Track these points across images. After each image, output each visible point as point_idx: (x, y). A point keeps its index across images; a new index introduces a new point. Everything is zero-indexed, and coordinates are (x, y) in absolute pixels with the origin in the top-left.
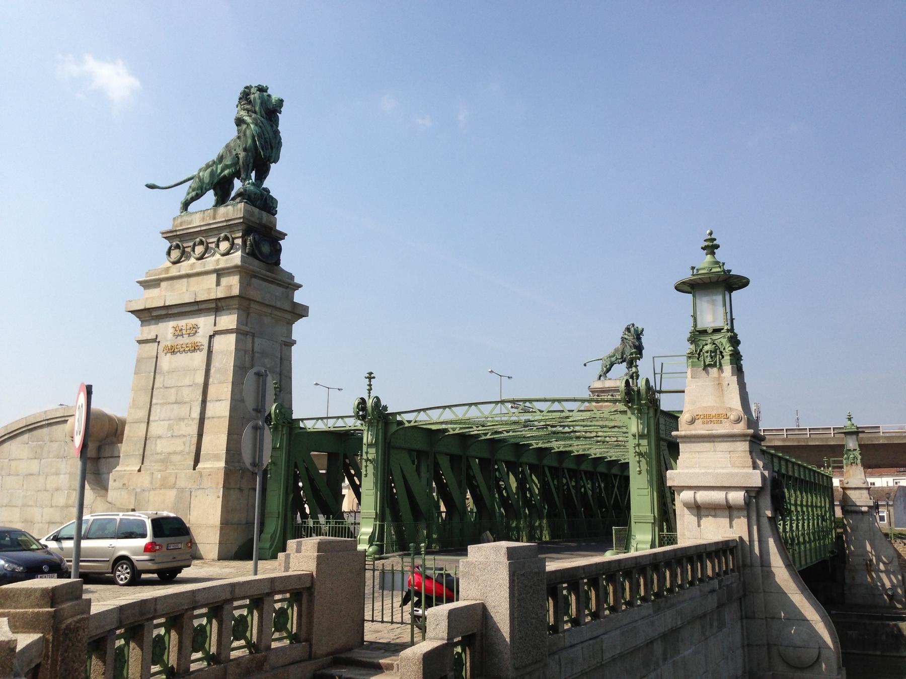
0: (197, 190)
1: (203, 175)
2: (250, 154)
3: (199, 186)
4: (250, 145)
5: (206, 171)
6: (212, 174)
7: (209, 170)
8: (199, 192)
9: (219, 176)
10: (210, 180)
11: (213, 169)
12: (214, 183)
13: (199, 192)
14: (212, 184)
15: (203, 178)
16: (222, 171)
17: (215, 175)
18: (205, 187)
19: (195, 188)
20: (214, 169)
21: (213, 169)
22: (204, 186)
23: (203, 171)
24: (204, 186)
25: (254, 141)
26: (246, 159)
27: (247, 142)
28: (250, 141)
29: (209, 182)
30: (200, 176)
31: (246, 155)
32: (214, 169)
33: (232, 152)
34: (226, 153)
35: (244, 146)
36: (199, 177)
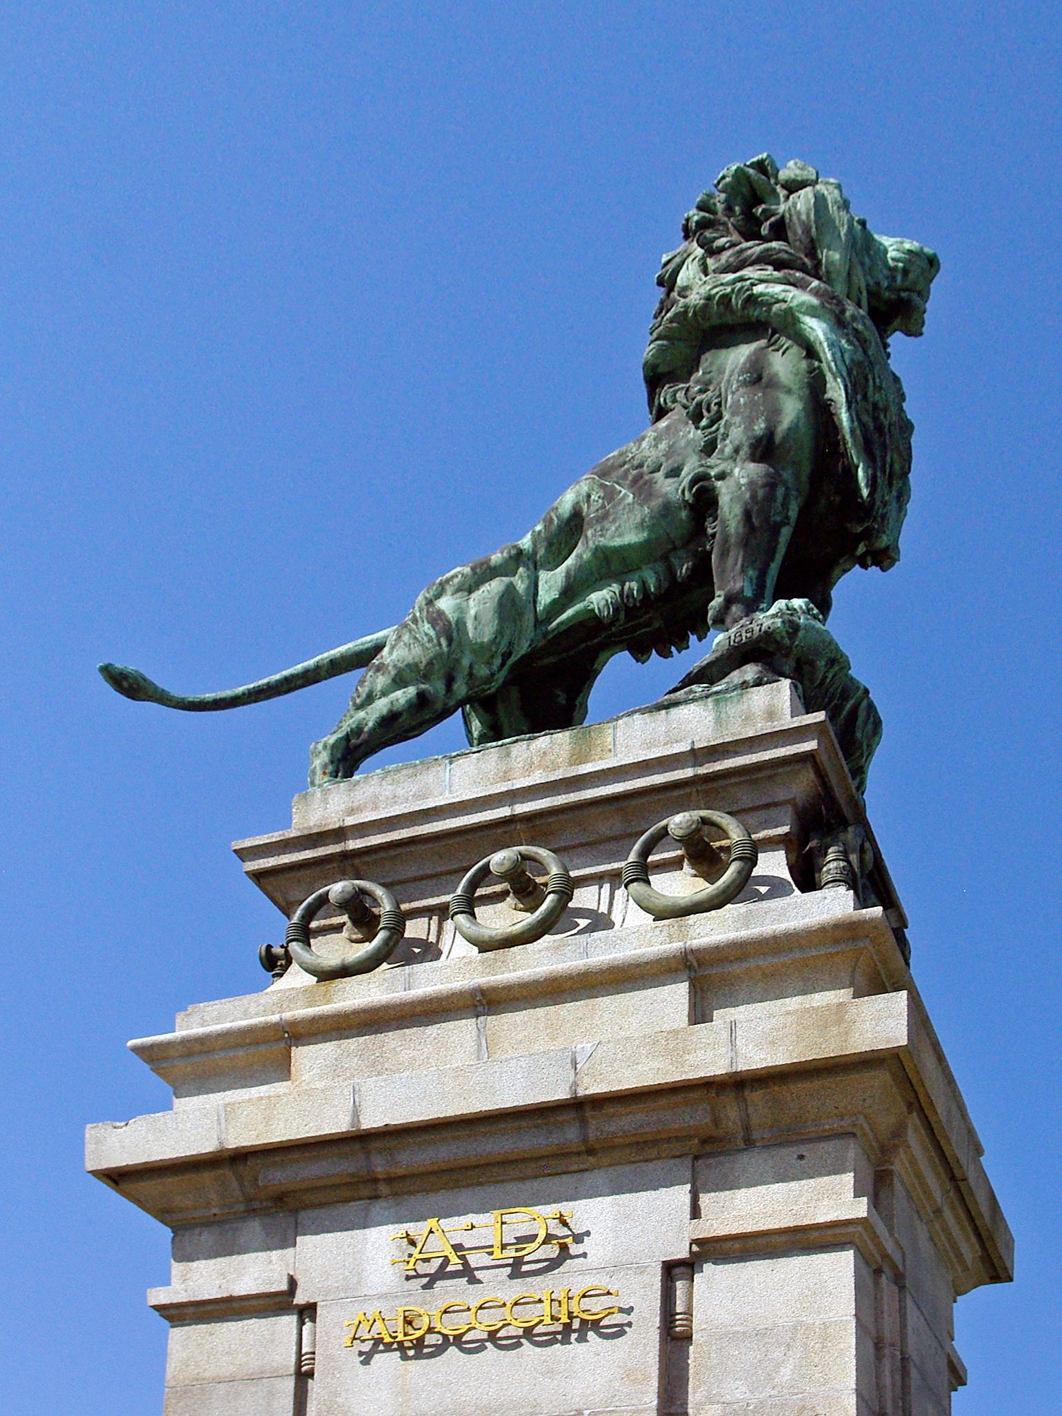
0: (426, 677)
1: (461, 610)
2: (787, 475)
3: (438, 656)
4: (793, 429)
5: (470, 591)
6: (509, 605)
7: (495, 586)
8: (436, 687)
9: (540, 622)
10: (499, 633)
11: (510, 589)
12: (513, 659)
13: (436, 687)
14: (506, 656)
15: (461, 623)
16: (570, 593)
17: (520, 615)
18: (471, 667)
19: (413, 667)
20: (521, 585)
21: (510, 588)
22: (466, 662)
23: (459, 590)
24: (466, 662)
25: (819, 408)
26: (770, 497)
27: (774, 414)
28: (791, 409)
29: (494, 641)
30: (441, 613)
31: (767, 475)
32: (521, 585)
33: (651, 483)
34: (610, 495)
35: (760, 427)
36: (437, 618)
